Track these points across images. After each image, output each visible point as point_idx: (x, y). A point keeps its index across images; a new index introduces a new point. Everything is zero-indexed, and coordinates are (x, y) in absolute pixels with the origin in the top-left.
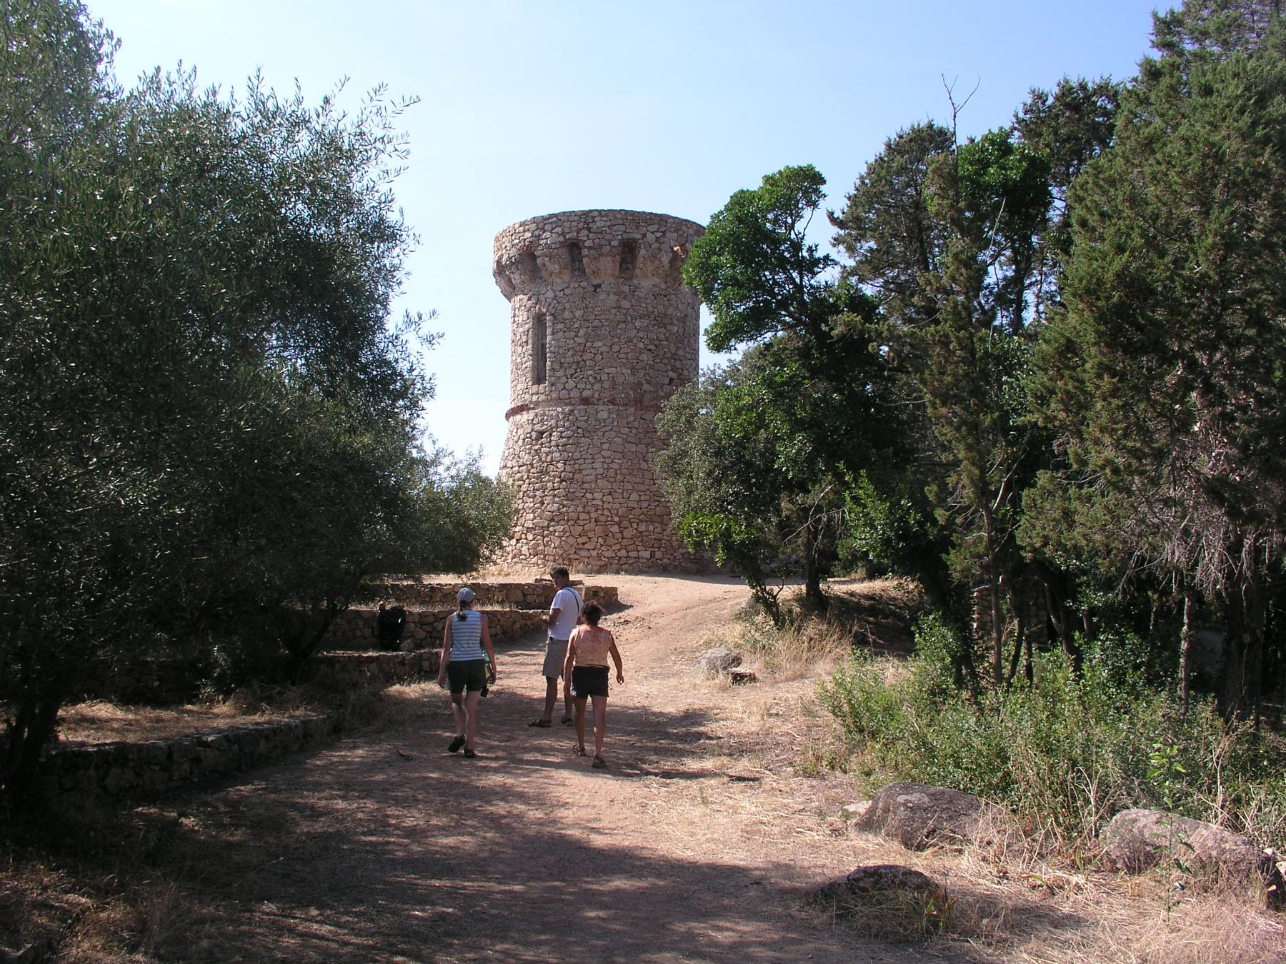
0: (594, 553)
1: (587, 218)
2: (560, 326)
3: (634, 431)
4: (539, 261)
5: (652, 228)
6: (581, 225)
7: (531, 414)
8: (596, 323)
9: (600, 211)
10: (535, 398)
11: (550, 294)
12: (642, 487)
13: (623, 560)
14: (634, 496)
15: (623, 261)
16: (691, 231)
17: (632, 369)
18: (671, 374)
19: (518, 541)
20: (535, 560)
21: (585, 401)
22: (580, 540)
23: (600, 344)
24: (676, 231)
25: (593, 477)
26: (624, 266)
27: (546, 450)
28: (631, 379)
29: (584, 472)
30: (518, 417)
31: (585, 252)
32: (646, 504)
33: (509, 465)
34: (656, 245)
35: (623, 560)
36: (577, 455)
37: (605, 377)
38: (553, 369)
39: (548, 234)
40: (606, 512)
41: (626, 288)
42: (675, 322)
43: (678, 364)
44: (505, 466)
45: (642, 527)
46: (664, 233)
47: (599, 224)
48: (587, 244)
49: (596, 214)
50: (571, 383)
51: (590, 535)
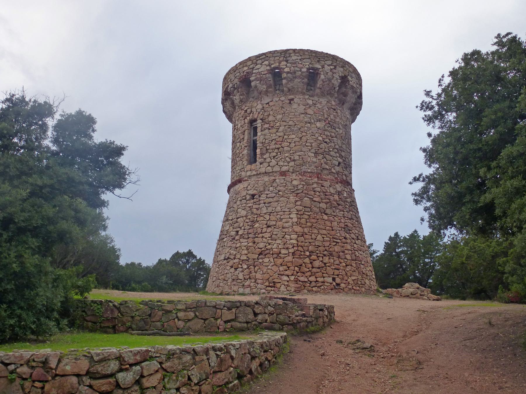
0: (292, 278)
1: (285, 54)
2: (267, 126)
4: (253, 84)
5: (329, 62)
6: (281, 59)
7: (245, 184)
8: (291, 123)
9: (294, 50)
10: (249, 173)
11: (260, 106)
12: (324, 232)
13: (313, 284)
14: (319, 237)
15: (308, 84)
16: (351, 70)
17: (316, 153)
18: (341, 160)
19: (236, 269)
21: (283, 174)
22: (281, 268)
23: (294, 136)
24: (343, 67)
25: (290, 224)
26: (309, 87)
27: (257, 206)
28: (315, 160)
29: (284, 220)
30: (237, 187)
31: (284, 75)
32: (327, 244)
33: (230, 218)
34: (330, 74)
35: (313, 284)
36: (279, 209)
37: (297, 158)
38: (262, 154)
39: (257, 67)
41: (310, 102)
42: (341, 127)
43: (343, 154)
44: (227, 220)
45: (326, 259)
46: (335, 67)
48: (287, 70)
49: (291, 52)
50: (274, 162)
51: (289, 264)
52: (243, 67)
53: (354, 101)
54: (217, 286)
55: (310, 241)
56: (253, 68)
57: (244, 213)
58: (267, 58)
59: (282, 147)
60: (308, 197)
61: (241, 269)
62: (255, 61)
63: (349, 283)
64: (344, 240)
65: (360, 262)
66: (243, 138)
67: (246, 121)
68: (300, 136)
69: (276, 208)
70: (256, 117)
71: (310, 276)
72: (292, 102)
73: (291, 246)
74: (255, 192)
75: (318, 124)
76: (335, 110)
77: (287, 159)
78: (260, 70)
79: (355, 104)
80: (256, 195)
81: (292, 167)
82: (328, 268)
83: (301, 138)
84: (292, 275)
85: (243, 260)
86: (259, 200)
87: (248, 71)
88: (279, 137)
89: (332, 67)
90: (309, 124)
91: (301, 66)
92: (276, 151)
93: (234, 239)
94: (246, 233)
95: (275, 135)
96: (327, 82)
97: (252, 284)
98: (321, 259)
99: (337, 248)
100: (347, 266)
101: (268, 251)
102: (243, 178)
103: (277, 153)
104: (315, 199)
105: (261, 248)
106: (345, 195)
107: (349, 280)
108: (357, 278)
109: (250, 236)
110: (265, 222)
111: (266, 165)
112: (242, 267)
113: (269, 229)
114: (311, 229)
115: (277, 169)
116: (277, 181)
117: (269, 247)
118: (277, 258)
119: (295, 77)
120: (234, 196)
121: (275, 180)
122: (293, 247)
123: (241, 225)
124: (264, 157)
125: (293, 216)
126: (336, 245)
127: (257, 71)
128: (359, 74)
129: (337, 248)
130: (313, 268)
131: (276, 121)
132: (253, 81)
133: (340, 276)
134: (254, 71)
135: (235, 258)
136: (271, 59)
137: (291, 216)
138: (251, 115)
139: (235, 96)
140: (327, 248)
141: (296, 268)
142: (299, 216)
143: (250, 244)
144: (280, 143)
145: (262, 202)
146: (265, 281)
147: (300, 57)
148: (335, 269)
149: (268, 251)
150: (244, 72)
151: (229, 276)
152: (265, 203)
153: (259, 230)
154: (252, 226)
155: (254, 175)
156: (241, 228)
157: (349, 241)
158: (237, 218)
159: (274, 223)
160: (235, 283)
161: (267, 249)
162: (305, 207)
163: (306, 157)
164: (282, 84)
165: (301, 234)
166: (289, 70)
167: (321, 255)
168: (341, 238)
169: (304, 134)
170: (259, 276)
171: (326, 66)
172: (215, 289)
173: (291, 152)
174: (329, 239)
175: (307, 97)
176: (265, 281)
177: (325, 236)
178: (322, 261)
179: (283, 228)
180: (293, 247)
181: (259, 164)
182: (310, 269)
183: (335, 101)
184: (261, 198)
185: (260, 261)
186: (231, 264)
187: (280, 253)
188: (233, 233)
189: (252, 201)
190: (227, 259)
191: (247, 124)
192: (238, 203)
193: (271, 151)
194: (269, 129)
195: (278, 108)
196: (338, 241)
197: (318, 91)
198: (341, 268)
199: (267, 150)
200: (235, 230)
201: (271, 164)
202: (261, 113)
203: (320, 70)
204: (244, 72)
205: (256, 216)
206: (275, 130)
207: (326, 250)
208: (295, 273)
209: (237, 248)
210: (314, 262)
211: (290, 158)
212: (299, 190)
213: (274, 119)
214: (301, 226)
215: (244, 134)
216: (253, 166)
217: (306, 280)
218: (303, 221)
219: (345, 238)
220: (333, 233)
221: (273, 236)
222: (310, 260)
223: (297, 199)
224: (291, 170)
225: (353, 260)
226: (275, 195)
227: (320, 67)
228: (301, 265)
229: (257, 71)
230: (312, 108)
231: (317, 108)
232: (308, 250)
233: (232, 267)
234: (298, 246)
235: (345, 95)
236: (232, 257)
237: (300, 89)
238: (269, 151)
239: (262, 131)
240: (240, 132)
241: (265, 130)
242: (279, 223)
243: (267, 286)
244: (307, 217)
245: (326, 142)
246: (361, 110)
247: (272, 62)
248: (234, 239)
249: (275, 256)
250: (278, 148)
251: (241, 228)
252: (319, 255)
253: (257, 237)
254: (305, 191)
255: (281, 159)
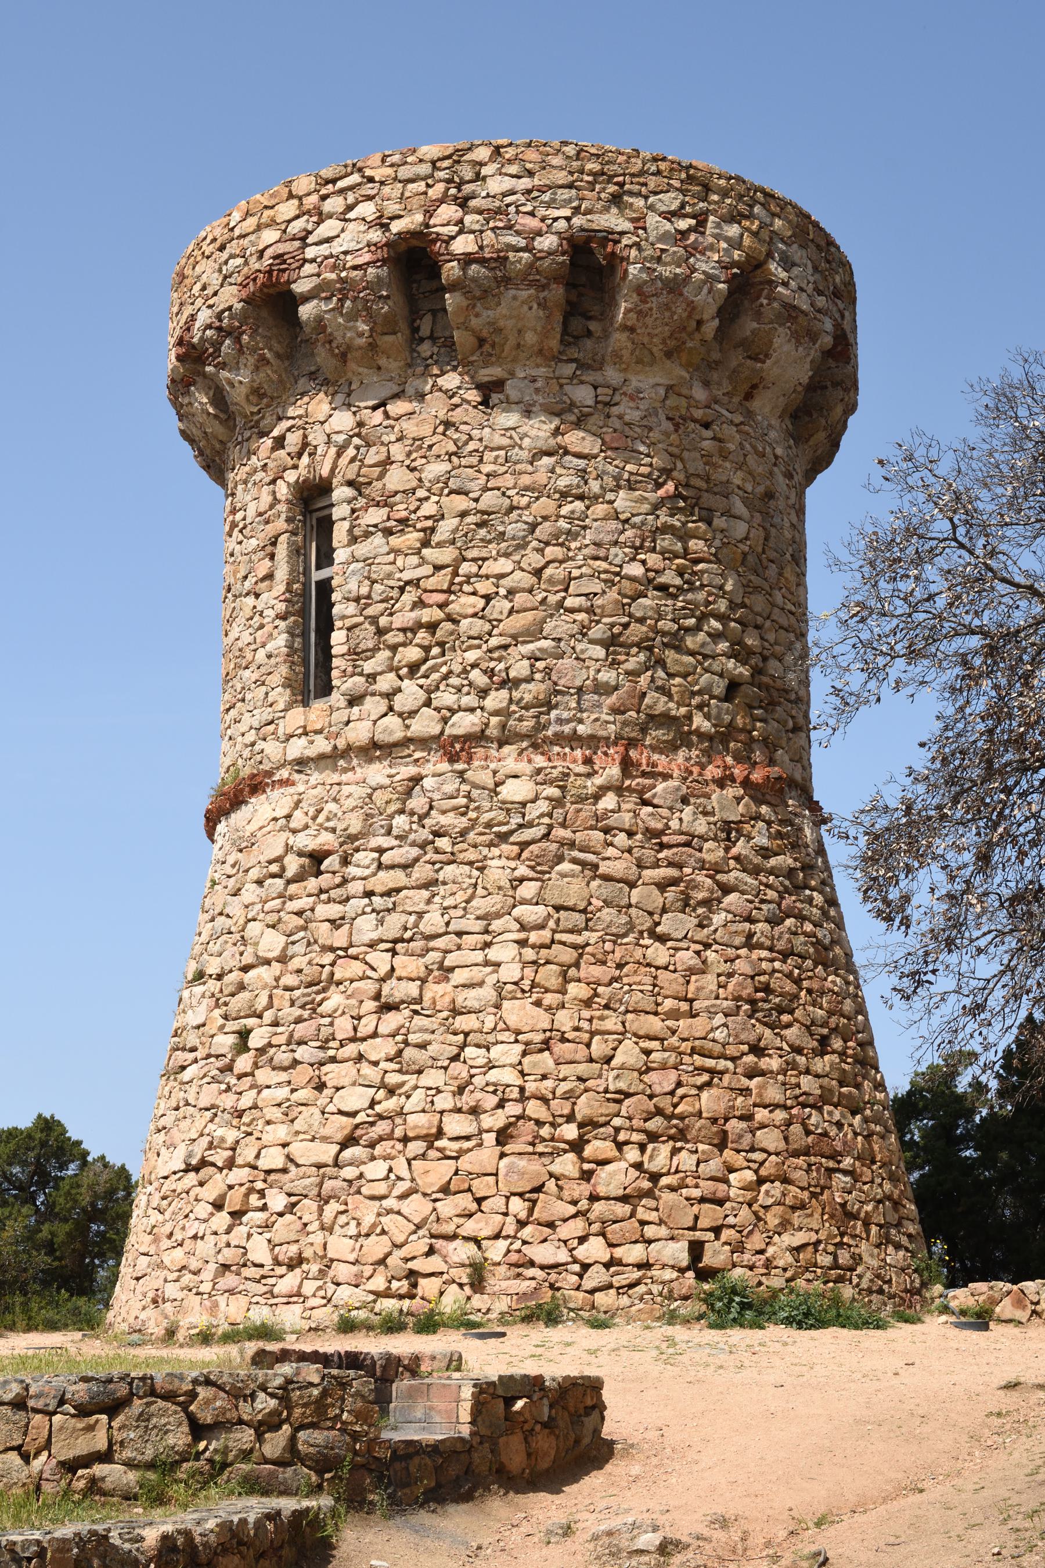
0: (496, 1251)
2: (375, 516)
3: (621, 839)
4: (306, 311)
8: (489, 500)
12: (655, 1024)
13: (596, 1277)
14: (628, 1053)
15: (572, 310)
17: (611, 643)
19: (237, 1215)
20: (289, 1282)
21: (458, 749)
22: (447, 1207)
23: (504, 565)
25: (487, 993)
27: (334, 910)
28: (607, 676)
29: (459, 976)
31: (451, 270)
33: (212, 969)
35: (596, 1277)
36: (433, 921)
37: (520, 669)
38: (355, 654)
40: (534, 1108)
41: (583, 395)
45: (660, 1157)
47: (496, 185)
49: (483, 153)
50: (411, 693)
51: (482, 1186)
52: (259, 228)
53: (803, 374)
54: (155, 1301)
55: (582, 1069)
56: (303, 239)
57: (272, 943)
58: (369, 189)
59: (450, 618)
60: (574, 861)
61: (259, 1217)
62: (314, 199)
63: (768, 1264)
64: (750, 1059)
65: (831, 1164)
66: (269, 576)
67: (283, 490)
68: (537, 560)
69: (420, 915)
70: (325, 472)
71: (582, 1240)
72: (495, 398)
73: (493, 1100)
74: (326, 840)
75: (623, 501)
76: (707, 426)
77: (476, 675)
78: (336, 248)
79: (815, 387)
80: (328, 853)
81: (496, 713)
82: (667, 1197)
83: (538, 573)
84: (497, 1236)
85: (268, 1172)
86: (345, 881)
87: (281, 248)
88: (438, 568)
89: (683, 224)
90: (579, 505)
91: (533, 223)
92: (422, 636)
93: (229, 1068)
94: (282, 1039)
95: (414, 560)
96: (663, 299)
97: (309, 1288)
98: (632, 1154)
99: (710, 1101)
100: (761, 1181)
101: (382, 1127)
102: (269, 774)
103: (427, 649)
104: (604, 868)
105: (353, 1114)
106: (764, 841)
107: (771, 1251)
108: (814, 1237)
109: (303, 1053)
110: (370, 987)
111: (374, 706)
112: (264, 1208)
113: (392, 1021)
114: (586, 1014)
115: (425, 724)
116: (428, 783)
117: (390, 1104)
118: (424, 1156)
119: (506, 281)
120: (231, 860)
121: (417, 780)
122: (501, 1105)
123: (263, 1001)
124: (368, 667)
125: (503, 952)
126: (708, 1084)
127: (324, 250)
128: (830, 243)
129: (710, 1101)
130: (594, 1198)
131: (421, 493)
132: (306, 298)
133: (726, 1234)
134: (310, 252)
135: (230, 1164)
136: (386, 190)
137: (493, 954)
138: (305, 459)
139: (223, 366)
140: (665, 1103)
141: (518, 1206)
142: (529, 954)
143: (301, 1095)
144: (440, 598)
145: (356, 887)
146: (368, 1270)
147: (525, 183)
148: (702, 1200)
149: (382, 1127)
150: (261, 253)
151: (206, 1248)
152: (369, 894)
153: (343, 1027)
154: (313, 1007)
155: (322, 757)
156: (260, 1017)
157: (773, 1063)
158: (245, 969)
159: (412, 989)
160: (230, 1280)
161: (381, 1117)
162: (558, 908)
163: (567, 662)
164: (445, 310)
165: (538, 1037)
166: (472, 248)
167: (636, 1137)
168: (731, 1051)
169: (551, 552)
170: (340, 1246)
171: (652, 220)
172: (143, 1316)
173: (494, 642)
174: (672, 1058)
175: (569, 369)
176: (368, 1270)
177: (655, 1045)
178: (638, 1166)
179: (456, 1012)
180: (501, 1105)
181: (343, 703)
182: (584, 1204)
183: (706, 384)
184: (352, 871)
185: (349, 1172)
186: (210, 1193)
187: (440, 1133)
188: (225, 1042)
189: (312, 884)
190: (197, 1169)
191: (282, 507)
192: (250, 893)
193: (400, 638)
194: (388, 532)
195: (426, 430)
196: (722, 1064)
197: (619, 339)
198: (733, 1193)
199: (380, 632)
200: (232, 1026)
201: (400, 702)
202: (351, 452)
203: (625, 241)
204: (261, 253)
205: (328, 958)
206: (413, 537)
207: (659, 1112)
208: (510, 1229)
209: (240, 1114)
210: (603, 1173)
211: (490, 673)
212: (530, 825)
213: (408, 480)
214: (538, 1003)
215: (272, 556)
216: (317, 712)
217: (563, 1256)
218: (549, 975)
219: (757, 1050)
220: (699, 1026)
221: (409, 1053)
222: (583, 1160)
223: (523, 871)
224: (493, 732)
225: (796, 1154)
226: (415, 852)
227: (628, 226)
228: (538, 1189)
229: (324, 250)
230: (596, 420)
231: (617, 424)
232: (570, 1118)
233: (218, 1205)
234: (523, 1097)
235: (758, 352)
236: (219, 1157)
237: (530, 338)
238: (391, 638)
239: (354, 540)
240: (254, 542)
241: (367, 535)
242: (433, 990)
243: (378, 1294)
244: (567, 955)
245: (663, 588)
246: (851, 408)
247: (392, 208)
248: (229, 1068)
249: (416, 1147)
250: (432, 627)
251: (260, 1017)
252: (622, 1137)
253: (333, 1060)
254: (559, 833)
255: (446, 677)
